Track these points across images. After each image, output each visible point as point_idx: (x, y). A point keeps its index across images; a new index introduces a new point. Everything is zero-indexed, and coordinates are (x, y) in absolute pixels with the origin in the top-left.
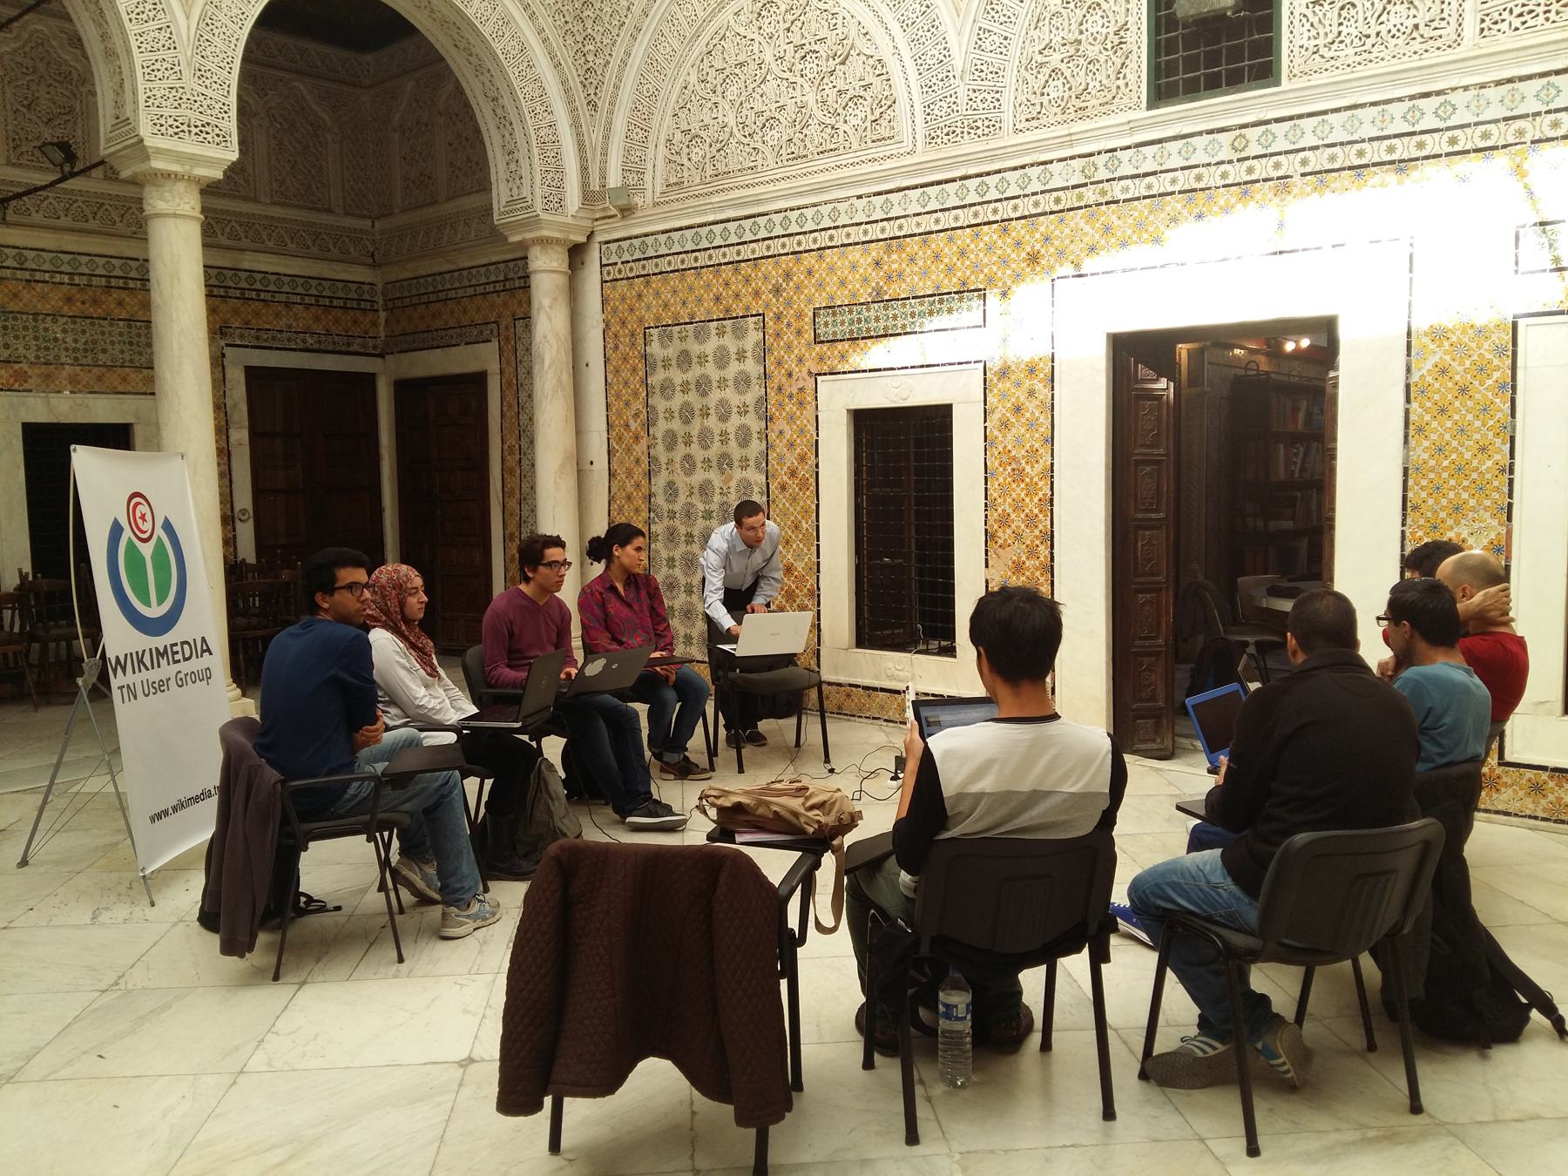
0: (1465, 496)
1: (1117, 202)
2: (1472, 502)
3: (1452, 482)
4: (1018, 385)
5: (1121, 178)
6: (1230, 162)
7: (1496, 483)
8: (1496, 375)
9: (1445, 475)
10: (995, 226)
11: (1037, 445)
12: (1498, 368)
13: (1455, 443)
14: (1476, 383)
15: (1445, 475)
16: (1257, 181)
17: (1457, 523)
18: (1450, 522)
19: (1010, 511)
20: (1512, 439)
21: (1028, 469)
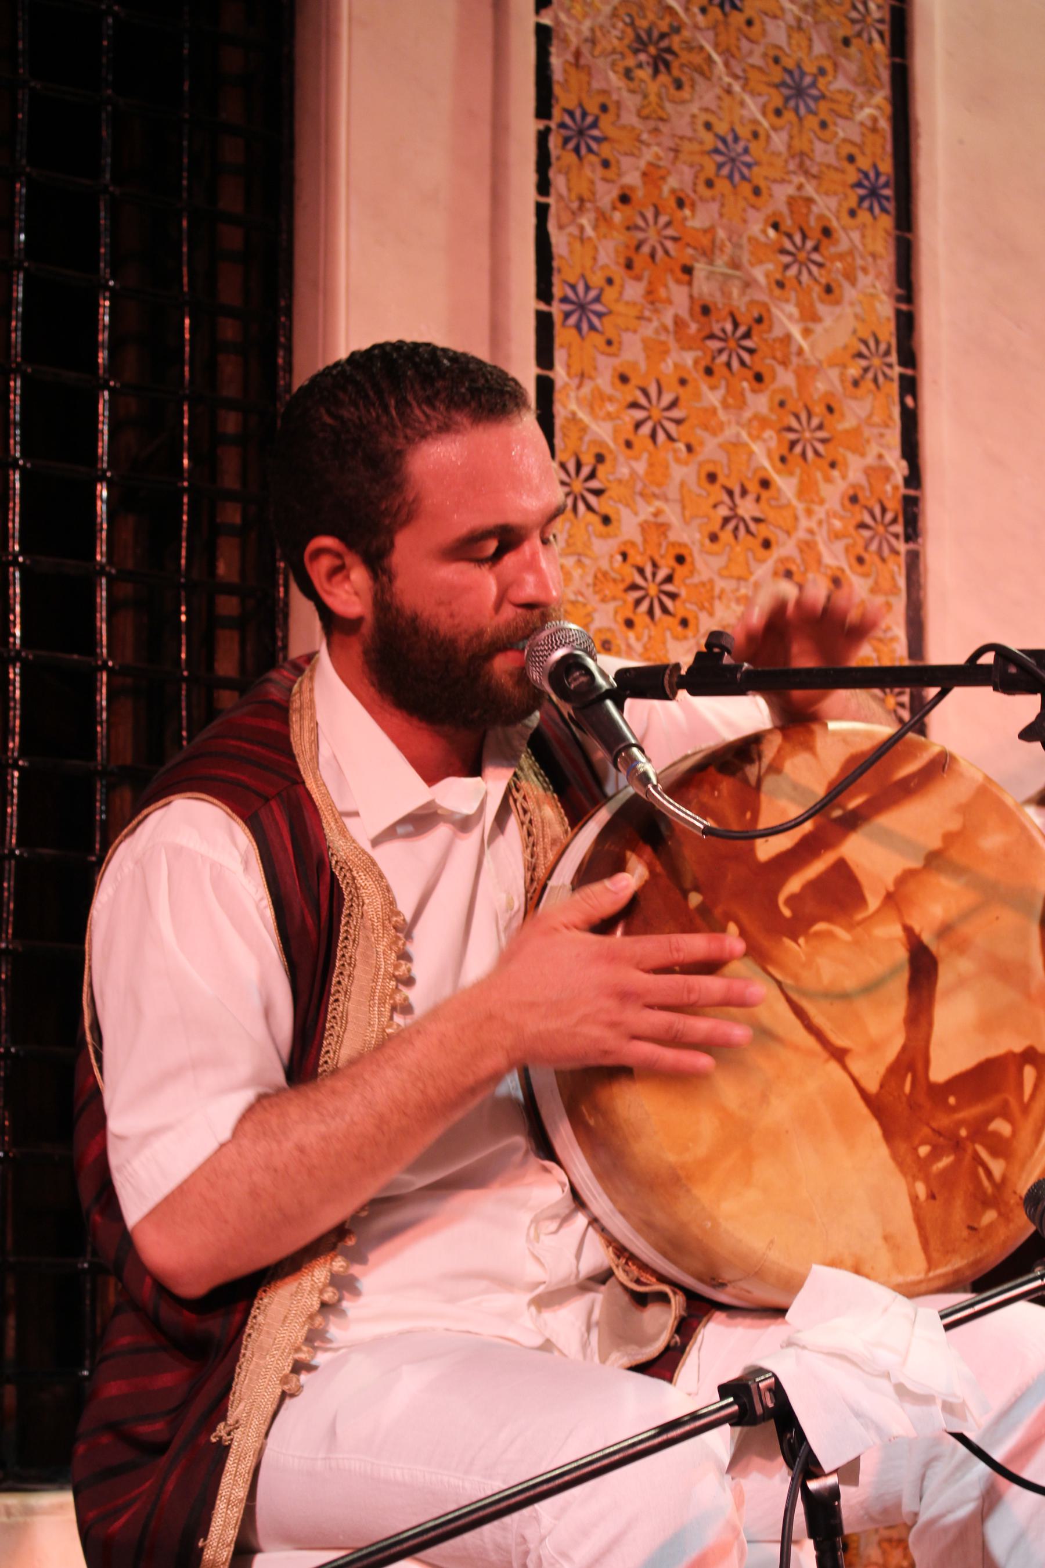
11: (827, 206)
19: (687, 534)
21: (786, 318)
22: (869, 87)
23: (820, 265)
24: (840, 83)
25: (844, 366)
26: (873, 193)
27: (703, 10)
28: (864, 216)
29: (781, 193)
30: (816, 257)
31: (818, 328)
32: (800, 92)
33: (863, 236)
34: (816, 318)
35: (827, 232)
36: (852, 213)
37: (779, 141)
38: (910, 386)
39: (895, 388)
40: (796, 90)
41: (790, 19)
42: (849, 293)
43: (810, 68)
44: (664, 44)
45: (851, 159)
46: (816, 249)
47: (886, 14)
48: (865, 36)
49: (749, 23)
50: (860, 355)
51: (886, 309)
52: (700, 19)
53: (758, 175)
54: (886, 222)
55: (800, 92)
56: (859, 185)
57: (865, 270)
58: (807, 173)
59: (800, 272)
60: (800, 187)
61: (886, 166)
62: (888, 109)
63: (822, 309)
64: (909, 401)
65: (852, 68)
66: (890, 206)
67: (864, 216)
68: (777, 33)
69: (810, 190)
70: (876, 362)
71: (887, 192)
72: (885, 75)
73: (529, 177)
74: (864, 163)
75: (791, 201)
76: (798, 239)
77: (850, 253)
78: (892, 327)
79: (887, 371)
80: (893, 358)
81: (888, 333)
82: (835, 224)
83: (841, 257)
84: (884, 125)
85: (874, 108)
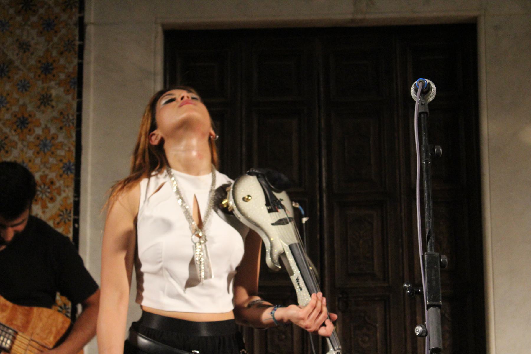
23: (49, 193)
25: (54, 220)
26: (69, 169)
27: (15, 131)
28: (65, 176)
30: (49, 190)
31: (47, 210)
32: (45, 145)
33: (64, 182)
34: (47, 207)
36: (61, 176)
38: (76, 221)
39: (72, 223)
41: (43, 126)
42: (59, 199)
44: (3, 142)
45: (61, 161)
46: (49, 188)
47: (75, 117)
48: (67, 125)
49: (30, 130)
50: (61, 215)
51: (71, 201)
52: (13, 133)
54: (72, 176)
55: (45, 145)
56: (64, 167)
57: (64, 191)
58: (47, 168)
59: (42, 196)
60: (44, 172)
61: (73, 160)
62: (74, 144)
63: (50, 205)
64: (76, 226)
66: (74, 171)
67: (65, 176)
69: (47, 172)
70: (66, 216)
71: (73, 167)
74: (65, 161)
76: (43, 186)
77: (60, 187)
78: (72, 206)
79: (69, 218)
80: (72, 214)
82: (55, 180)
83: (56, 189)
84: (73, 149)
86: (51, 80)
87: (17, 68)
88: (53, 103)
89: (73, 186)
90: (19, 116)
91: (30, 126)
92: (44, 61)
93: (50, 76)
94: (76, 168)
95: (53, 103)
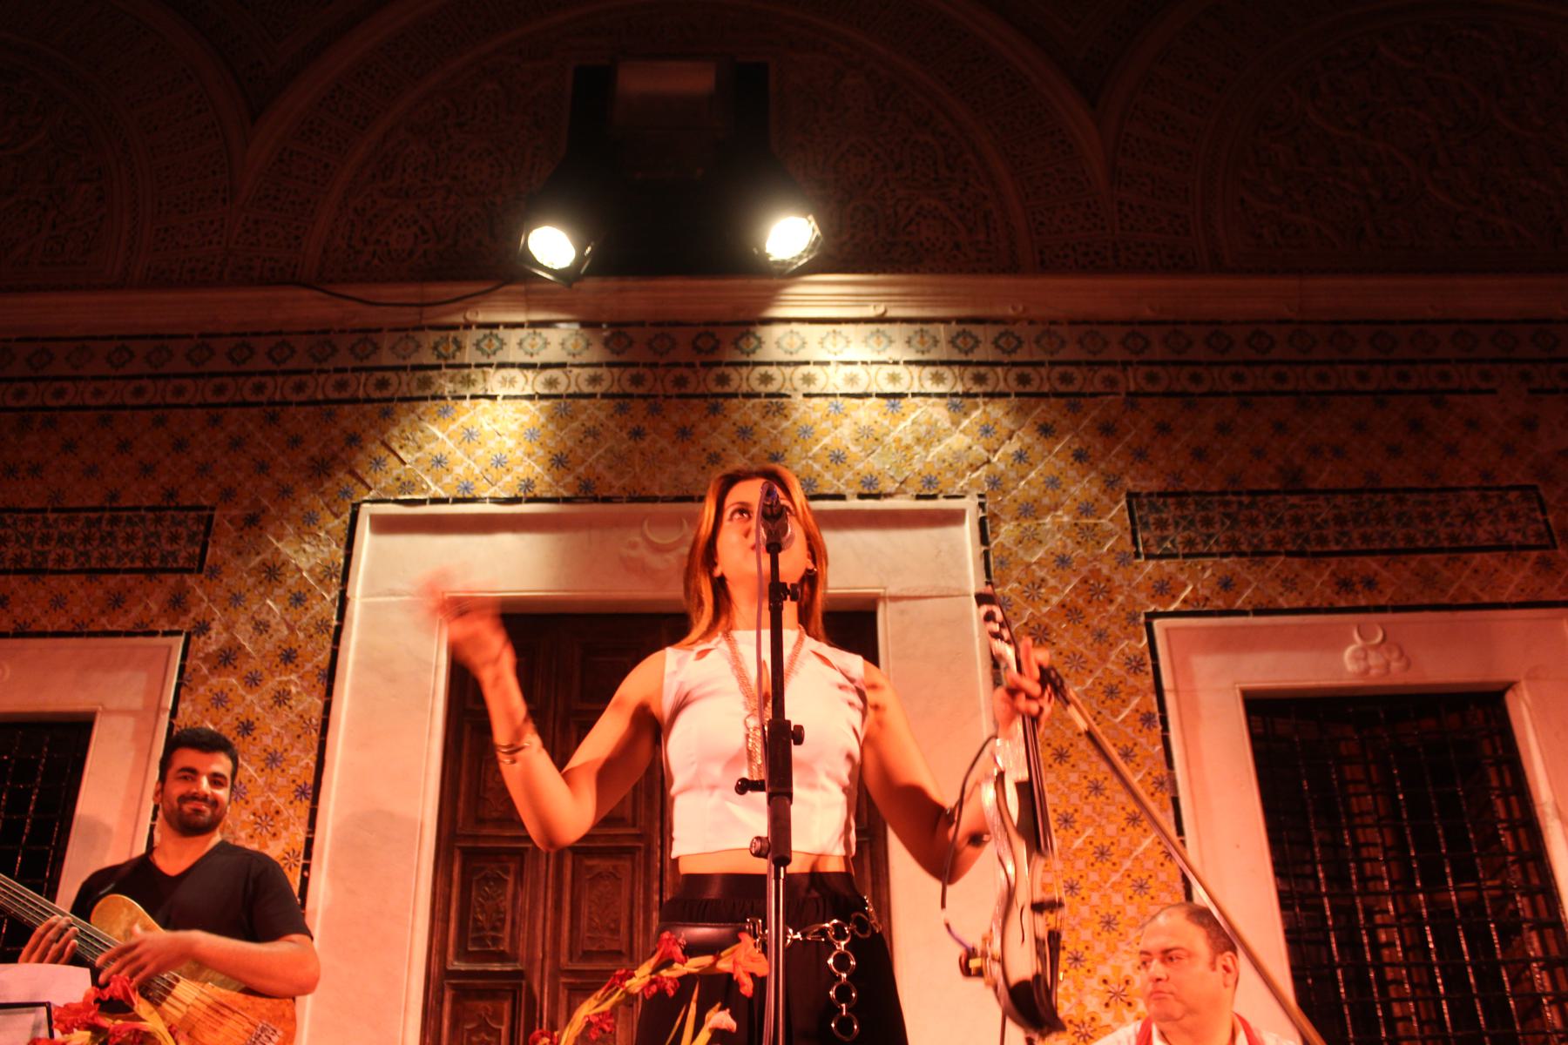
0: (1117, 899)
1: (493, 398)
2: (1131, 910)
3: (1094, 877)
4: (253, 681)
5: (502, 366)
6: (690, 365)
7: (1163, 876)
8: (1135, 701)
9: (1080, 864)
10: (254, 411)
11: (279, 802)
12: (1135, 691)
13: (1087, 810)
14: (1104, 712)
15: (1080, 864)
16: (735, 395)
17: (1113, 950)
18: (1100, 947)
20: (1175, 802)
22: (306, 751)
24: (295, 752)
26: (303, 792)
28: (297, 803)
29: (258, 801)
32: (274, 760)
35: (278, 812)
37: (261, 781)
38: (306, 867)
40: (273, 760)
42: (284, 834)
43: (280, 750)
51: (301, 837)
53: (248, 797)
54: (307, 803)
55: (274, 760)
61: (310, 781)
65: (300, 746)
68: (267, 740)
69: (272, 796)
72: (316, 745)
73: (150, 814)
74: (300, 782)
75: (263, 804)
81: (301, 847)
84: (312, 765)
85: (310, 760)
86: (292, 671)
87: (248, 655)
88: (293, 703)
89: (306, 816)
90: (243, 719)
91: (255, 733)
92: (285, 646)
93: (291, 666)
94: (313, 792)
95: (293, 703)
